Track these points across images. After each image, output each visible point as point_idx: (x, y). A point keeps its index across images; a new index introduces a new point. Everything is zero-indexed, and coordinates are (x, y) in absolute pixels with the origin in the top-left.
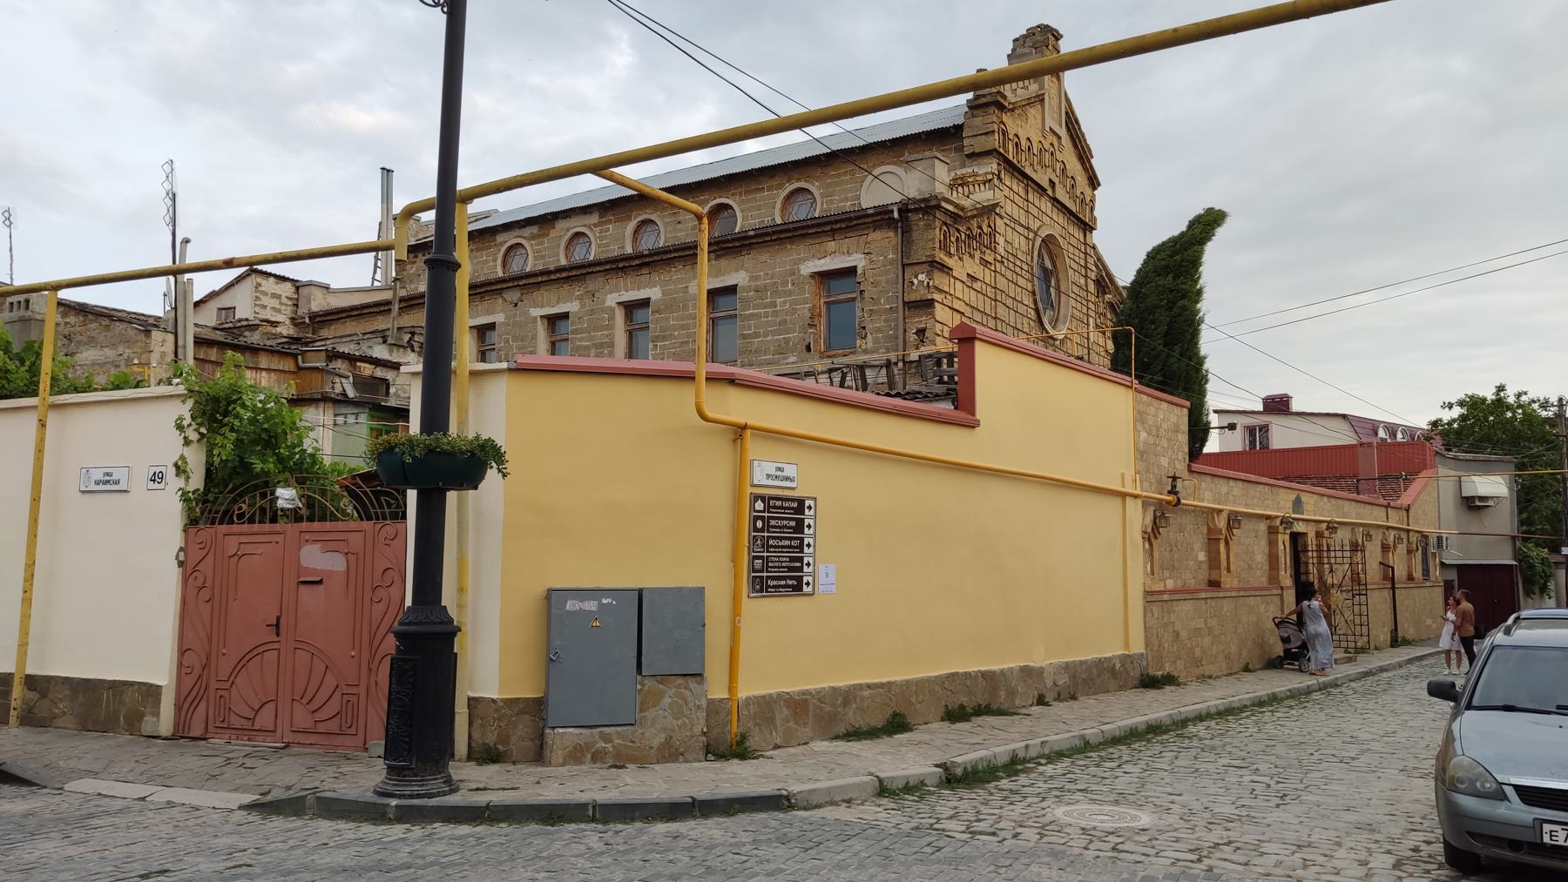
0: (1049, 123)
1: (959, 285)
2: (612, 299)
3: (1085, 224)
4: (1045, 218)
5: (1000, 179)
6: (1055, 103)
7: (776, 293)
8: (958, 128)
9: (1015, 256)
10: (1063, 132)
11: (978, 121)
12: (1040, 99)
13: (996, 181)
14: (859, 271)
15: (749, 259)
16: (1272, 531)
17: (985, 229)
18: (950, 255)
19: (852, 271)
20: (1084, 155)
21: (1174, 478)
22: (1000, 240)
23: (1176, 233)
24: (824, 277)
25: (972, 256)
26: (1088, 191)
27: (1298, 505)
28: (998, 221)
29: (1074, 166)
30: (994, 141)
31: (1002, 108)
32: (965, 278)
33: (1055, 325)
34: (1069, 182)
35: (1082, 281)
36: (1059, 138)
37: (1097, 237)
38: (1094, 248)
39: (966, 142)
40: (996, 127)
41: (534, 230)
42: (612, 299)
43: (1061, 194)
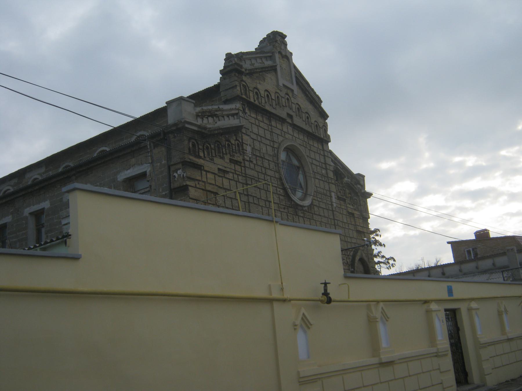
0: (281, 82)
1: (210, 176)
2: (27, 211)
4: (287, 136)
5: (244, 111)
10: (295, 88)
12: (273, 69)
13: (241, 114)
14: (148, 174)
16: (428, 312)
17: (233, 142)
18: (200, 157)
19: (143, 175)
20: (314, 100)
21: (326, 284)
22: (249, 149)
23: (211, 86)
25: (222, 158)
26: (320, 120)
27: (450, 291)
30: (238, 91)
31: (241, 73)
32: (216, 171)
33: (303, 199)
34: (304, 116)
35: (324, 172)
36: (292, 91)
37: (332, 146)
38: (331, 152)
39: (222, 94)
40: (237, 83)
41: (15, 181)
43: (297, 121)
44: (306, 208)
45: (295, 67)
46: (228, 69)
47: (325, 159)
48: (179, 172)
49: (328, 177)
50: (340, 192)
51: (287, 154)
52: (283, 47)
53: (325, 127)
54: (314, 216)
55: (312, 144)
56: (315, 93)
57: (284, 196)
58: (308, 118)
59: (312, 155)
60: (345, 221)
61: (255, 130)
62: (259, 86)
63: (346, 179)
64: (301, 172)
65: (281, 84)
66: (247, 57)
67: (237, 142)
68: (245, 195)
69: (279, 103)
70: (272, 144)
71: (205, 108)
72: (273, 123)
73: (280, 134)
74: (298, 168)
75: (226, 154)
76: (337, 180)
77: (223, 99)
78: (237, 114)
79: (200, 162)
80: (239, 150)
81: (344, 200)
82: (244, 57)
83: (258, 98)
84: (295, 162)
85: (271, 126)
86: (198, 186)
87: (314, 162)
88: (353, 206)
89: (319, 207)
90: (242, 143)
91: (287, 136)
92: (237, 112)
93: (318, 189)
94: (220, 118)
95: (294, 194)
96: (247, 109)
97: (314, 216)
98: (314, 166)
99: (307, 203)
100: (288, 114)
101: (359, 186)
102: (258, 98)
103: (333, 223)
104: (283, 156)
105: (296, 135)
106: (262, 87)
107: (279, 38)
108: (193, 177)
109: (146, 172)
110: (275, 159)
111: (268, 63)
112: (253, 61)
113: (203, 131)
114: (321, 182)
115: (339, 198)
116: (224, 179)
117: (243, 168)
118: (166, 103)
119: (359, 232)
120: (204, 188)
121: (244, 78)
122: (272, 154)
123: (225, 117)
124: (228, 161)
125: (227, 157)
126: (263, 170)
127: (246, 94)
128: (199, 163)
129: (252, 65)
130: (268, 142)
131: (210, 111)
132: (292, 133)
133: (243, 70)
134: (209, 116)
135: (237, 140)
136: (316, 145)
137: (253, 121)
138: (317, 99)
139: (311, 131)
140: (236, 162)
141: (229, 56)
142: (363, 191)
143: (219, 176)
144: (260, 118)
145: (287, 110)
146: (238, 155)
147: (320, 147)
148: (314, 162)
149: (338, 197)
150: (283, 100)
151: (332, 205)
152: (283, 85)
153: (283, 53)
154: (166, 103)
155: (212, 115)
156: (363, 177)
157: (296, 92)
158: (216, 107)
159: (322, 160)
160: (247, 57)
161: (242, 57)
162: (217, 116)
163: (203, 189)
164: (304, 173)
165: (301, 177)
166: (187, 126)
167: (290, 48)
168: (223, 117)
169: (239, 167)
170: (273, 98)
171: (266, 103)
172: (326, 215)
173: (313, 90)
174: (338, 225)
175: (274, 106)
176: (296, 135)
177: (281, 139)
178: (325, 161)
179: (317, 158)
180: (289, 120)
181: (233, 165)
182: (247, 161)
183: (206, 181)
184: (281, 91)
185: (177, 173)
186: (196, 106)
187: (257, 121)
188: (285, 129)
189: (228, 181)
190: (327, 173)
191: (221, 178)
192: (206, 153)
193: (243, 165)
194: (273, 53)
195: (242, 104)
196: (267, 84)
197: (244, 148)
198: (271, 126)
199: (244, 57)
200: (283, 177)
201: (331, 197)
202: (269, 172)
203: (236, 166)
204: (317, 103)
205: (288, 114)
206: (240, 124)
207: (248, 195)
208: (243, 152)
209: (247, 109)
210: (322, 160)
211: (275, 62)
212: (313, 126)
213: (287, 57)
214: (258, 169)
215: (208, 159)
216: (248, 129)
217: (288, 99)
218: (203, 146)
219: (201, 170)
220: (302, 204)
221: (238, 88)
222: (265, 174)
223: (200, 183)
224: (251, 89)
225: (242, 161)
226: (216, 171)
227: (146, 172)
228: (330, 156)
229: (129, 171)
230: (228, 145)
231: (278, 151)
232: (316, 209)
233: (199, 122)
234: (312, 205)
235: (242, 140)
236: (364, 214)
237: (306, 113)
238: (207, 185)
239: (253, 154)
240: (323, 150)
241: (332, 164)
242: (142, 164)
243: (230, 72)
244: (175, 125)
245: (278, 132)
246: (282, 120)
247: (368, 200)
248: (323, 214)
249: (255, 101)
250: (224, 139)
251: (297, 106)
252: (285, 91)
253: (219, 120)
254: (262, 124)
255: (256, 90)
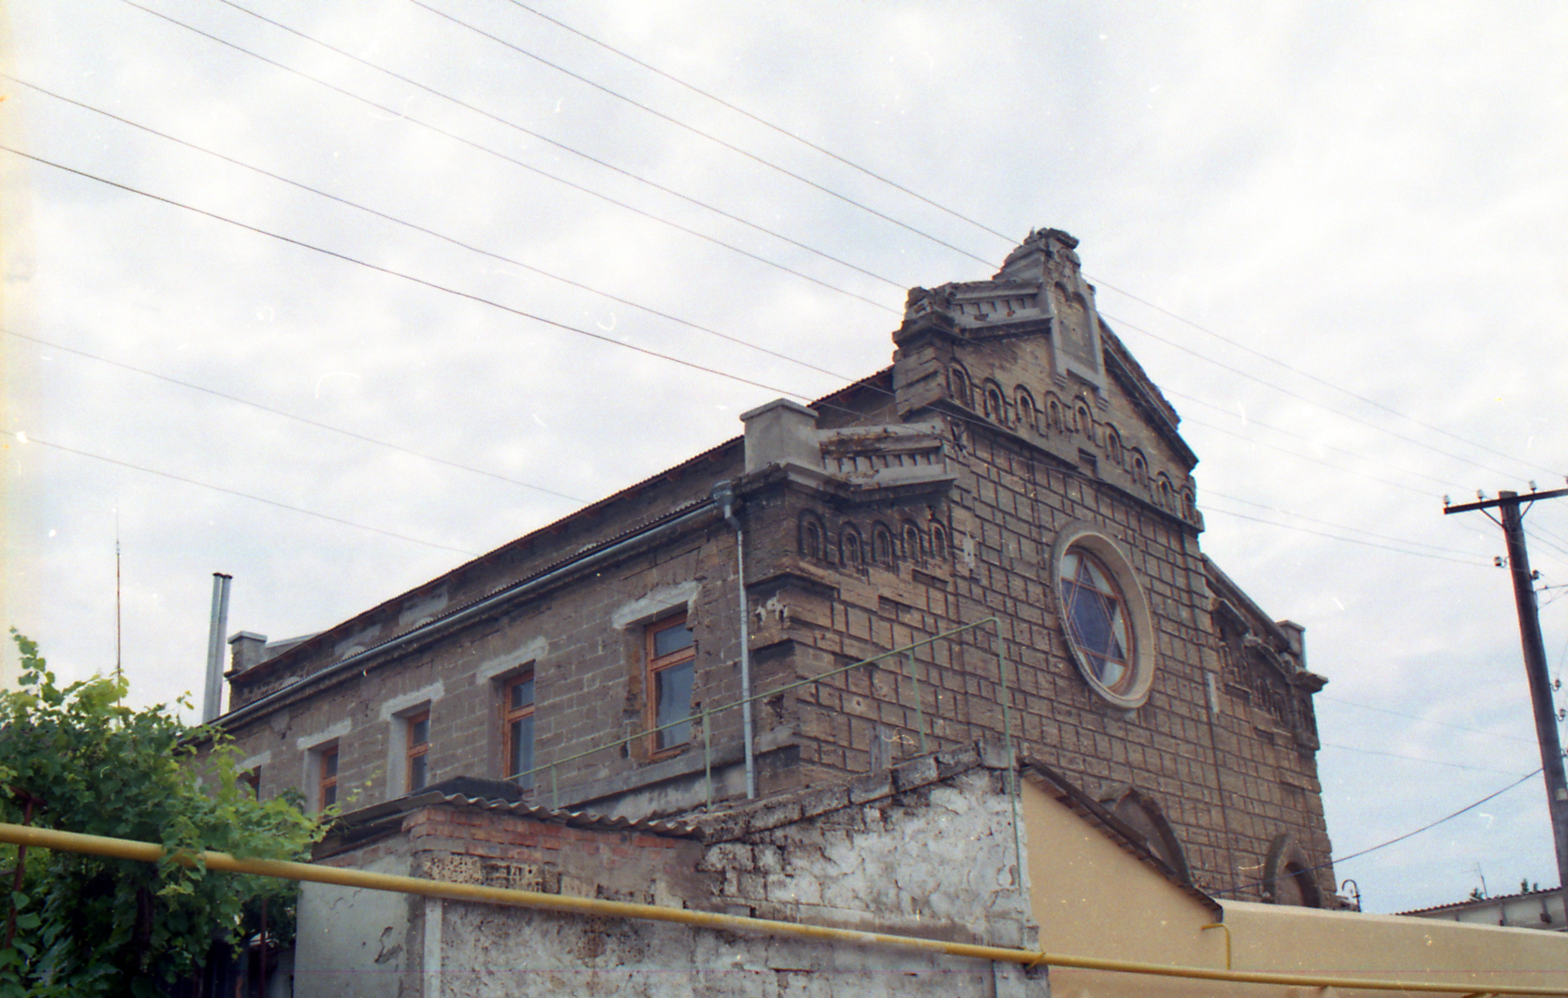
0: (1064, 363)
3: (1180, 524)
4: (1079, 512)
6: (1077, 337)
7: (583, 666)
8: (885, 378)
9: (1008, 572)
10: (1101, 379)
11: (912, 361)
12: (1041, 329)
15: (547, 620)
18: (831, 565)
19: (678, 613)
20: (1160, 419)
24: (646, 627)
25: (893, 569)
26: (1174, 471)
28: (959, 513)
29: (1134, 430)
32: (874, 605)
34: (1130, 458)
35: (1185, 614)
36: (1094, 389)
37: (1210, 544)
38: (1205, 561)
39: (900, 396)
42: (389, 707)
44: (1133, 715)
45: (1102, 325)
46: (915, 328)
47: (1188, 578)
48: (769, 603)
49: (1196, 629)
50: (1232, 672)
51: (1081, 561)
52: (1067, 271)
53: (1188, 491)
54: (1157, 738)
55: (1151, 535)
56: (1159, 396)
57: (1068, 678)
58: (1139, 463)
59: (1153, 570)
60: (1247, 754)
61: (988, 493)
62: (1000, 376)
63: (1249, 637)
64: (1118, 611)
65: (1062, 369)
66: (969, 295)
67: (935, 525)
68: (955, 672)
69: (1056, 422)
70: (1034, 534)
71: (847, 432)
72: (1040, 478)
73: (1058, 505)
74: (1112, 603)
75: (904, 558)
76: (1222, 639)
77: (902, 410)
78: (937, 450)
79: (828, 576)
80: (941, 548)
81: (1245, 697)
82: (959, 296)
83: (996, 408)
84: (1104, 587)
85: (1035, 484)
86: (821, 644)
87: (1158, 586)
88: (1269, 711)
89: (1171, 713)
90: (951, 528)
91: (1079, 512)
92: (937, 443)
93: (1169, 663)
94: (890, 459)
95: (1099, 673)
96: (964, 437)
97: (1157, 738)
98: (1157, 599)
99: (1136, 697)
100: (1081, 451)
101: (1287, 657)
102: (996, 408)
103: (1211, 761)
104: (1067, 567)
105: (1104, 510)
106: (1007, 380)
107: (1055, 247)
108: (808, 617)
109: (685, 604)
110: (1044, 575)
111: (1025, 313)
112: (985, 308)
113: (842, 494)
114: (1178, 644)
115: (1228, 690)
116: (897, 628)
117: (950, 598)
118: (748, 418)
119: (1285, 785)
120: (837, 649)
121: (959, 353)
122: (1034, 561)
123: (904, 458)
124: (909, 578)
125: (906, 567)
126: (1009, 604)
127: (962, 395)
128: (826, 581)
129: (982, 317)
130: (1024, 529)
131: (861, 441)
132: (1094, 506)
133: (956, 331)
134: (858, 454)
135: (934, 519)
136: (1163, 540)
137: (982, 468)
138: (1165, 414)
139: (1147, 499)
140: (933, 581)
141: (917, 297)
142: (1298, 669)
143: (882, 618)
144: (1001, 462)
145: (1080, 441)
146: (938, 560)
147: (1175, 545)
148: (1158, 586)
149: (1226, 685)
150: (1069, 414)
151: (1208, 707)
152: (1069, 372)
153: (1070, 289)
154: (748, 418)
155: (868, 450)
156: (1300, 631)
157: (1104, 394)
158: (878, 429)
159: (1181, 582)
160: (969, 295)
161: (952, 294)
162: (882, 455)
163: (834, 653)
164: (1128, 616)
165: (1119, 625)
166: (793, 477)
167: (1088, 273)
168: (898, 457)
169: (939, 596)
170: (1040, 406)
171: (1019, 419)
172: (1191, 735)
173: (1153, 388)
174: (1224, 765)
175: (1043, 428)
176: (1104, 510)
177: (1061, 519)
178: (1189, 584)
179: (1167, 575)
180: (1087, 471)
181: (922, 588)
182: (963, 578)
183: (843, 629)
184: (1062, 388)
185: (764, 606)
186: (820, 424)
187: (994, 470)
188: (1074, 494)
189: (906, 631)
190: (1194, 620)
191: (887, 625)
192: (847, 554)
193: (950, 588)
194: (1039, 286)
195: (954, 424)
196: (1026, 371)
197: (956, 542)
198: (1035, 484)
199: (959, 296)
200: (1066, 625)
201: (1205, 684)
202: (1025, 612)
203: (933, 593)
204: (1165, 423)
205: (1081, 451)
206: (943, 478)
207: (963, 674)
208: (953, 554)
209: (964, 440)
210: (1181, 582)
211: (1046, 310)
212: (1153, 485)
213: (1081, 298)
214: (994, 600)
215: (850, 570)
216: (968, 492)
217: (1082, 411)
218: (840, 535)
219: (831, 599)
220: (1117, 702)
221: (941, 379)
222: (1014, 616)
223: (828, 635)
224: (976, 381)
225: (950, 579)
226: (874, 605)
227: (685, 604)
228: (1202, 570)
229: (643, 602)
230: (911, 533)
231: (1052, 556)
232: (1161, 717)
233: (831, 468)
234: (1148, 709)
235: (950, 519)
236: (1305, 735)
237: (1136, 449)
238: (847, 641)
239: (978, 557)
240: (1184, 554)
241: (1208, 593)
242: (676, 583)
243: (921, 334)
244: (763, 475)
245: (1055, 501)
246: (1066, 469)
247: (1315, 697)
248: (1180, 734)
249: (987, 415)
250: (897, 516)
251: (1108, 431)
252: (1075, 389)
253: (887, 466)
254: (1007, 479)
255: (990, 386)
